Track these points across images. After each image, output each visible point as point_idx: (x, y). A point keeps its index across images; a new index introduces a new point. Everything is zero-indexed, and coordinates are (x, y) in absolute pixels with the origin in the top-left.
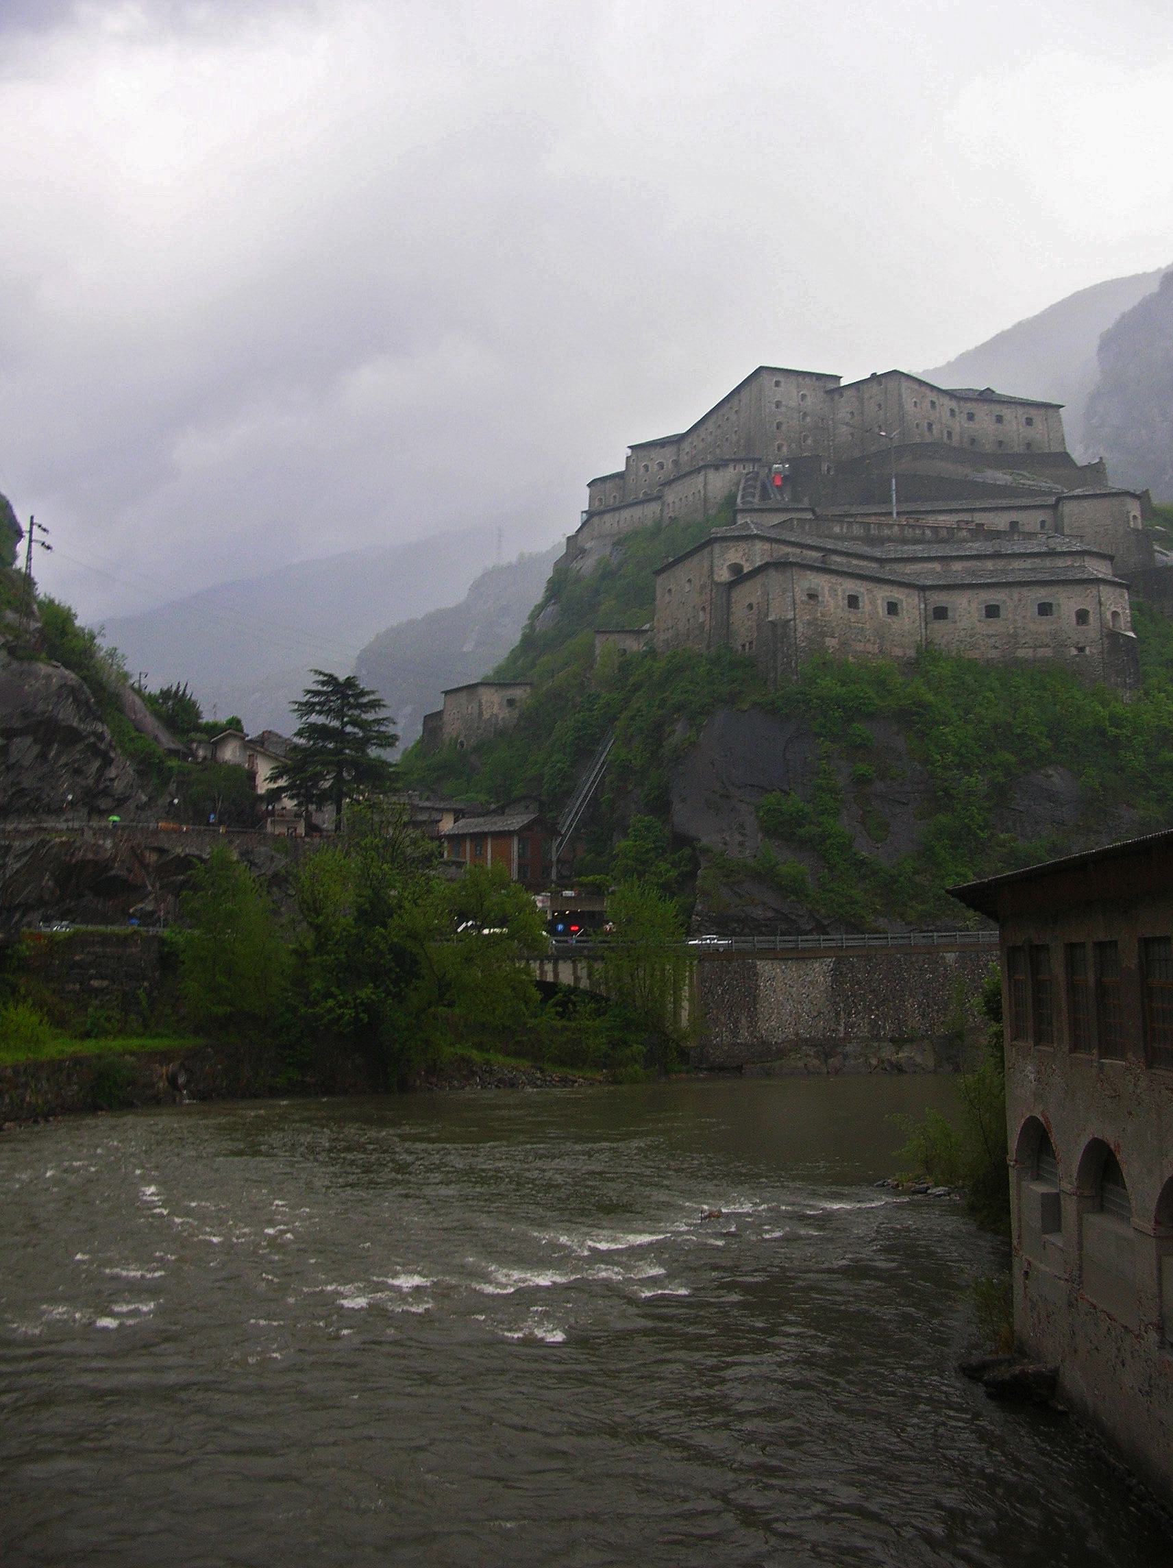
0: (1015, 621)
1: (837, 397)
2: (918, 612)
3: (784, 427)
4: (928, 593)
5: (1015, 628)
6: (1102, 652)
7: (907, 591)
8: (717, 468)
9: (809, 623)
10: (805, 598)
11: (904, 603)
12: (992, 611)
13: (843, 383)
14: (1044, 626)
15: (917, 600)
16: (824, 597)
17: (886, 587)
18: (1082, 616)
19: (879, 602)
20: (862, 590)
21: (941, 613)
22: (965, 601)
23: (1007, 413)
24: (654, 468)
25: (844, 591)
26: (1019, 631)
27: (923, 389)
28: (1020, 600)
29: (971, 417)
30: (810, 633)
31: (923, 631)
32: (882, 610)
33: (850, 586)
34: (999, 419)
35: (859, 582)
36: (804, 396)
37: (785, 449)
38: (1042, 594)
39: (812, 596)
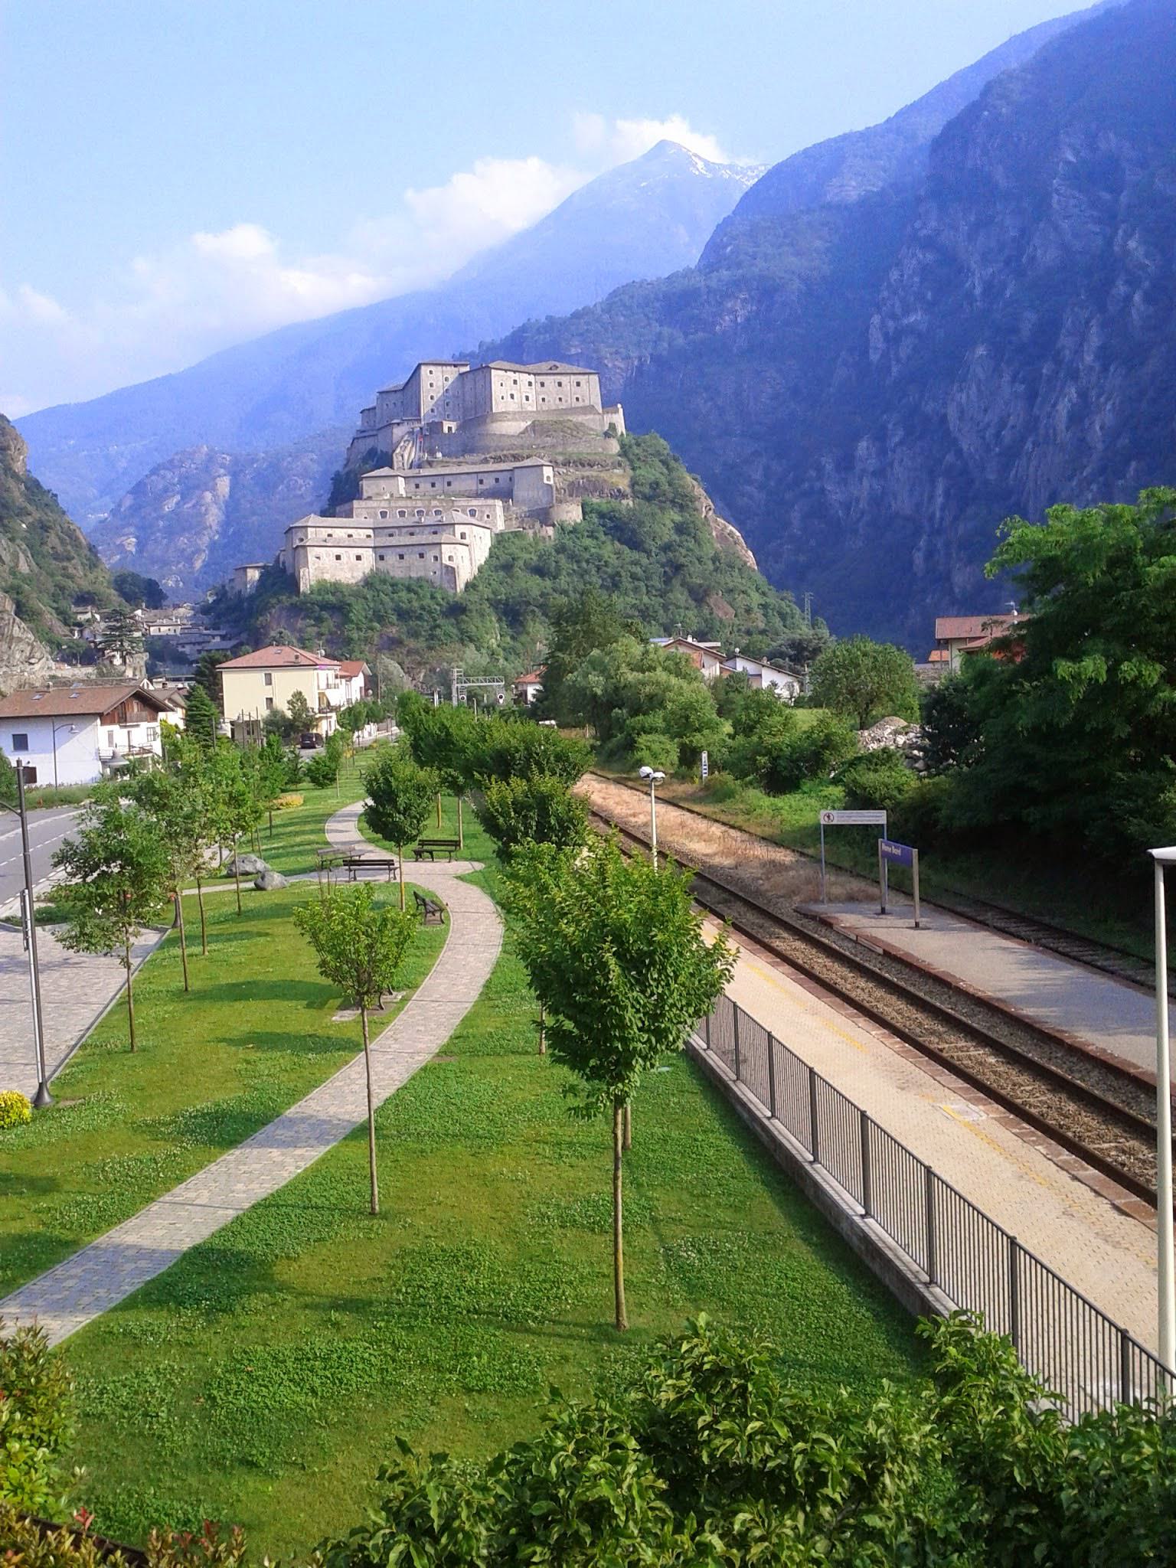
8: (398, 424)
18: (436, 558)
23: (564, 379)
24: (391, 406)
29: (542, 384)
33: (337, 551)
34: (560, 384)
38: (420, 549)
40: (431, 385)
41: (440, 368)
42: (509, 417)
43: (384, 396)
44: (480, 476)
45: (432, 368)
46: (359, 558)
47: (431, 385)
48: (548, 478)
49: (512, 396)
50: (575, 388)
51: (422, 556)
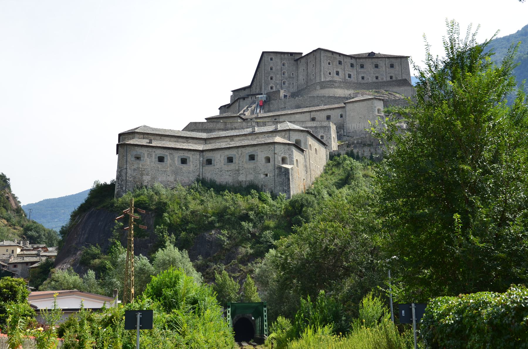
0: (239, 163)
1: (299, 62)
2: (198, 162)
3: (274, 78)
4: (204, 153)
5: (239, 166)
6: (274, 176)
7: (193, 153)
9: (135, 170)
10: (133, 159)
11: (191, 159)
12: (230, 160)
13: (303, 55)
14: (251, 165)
15: (198, 156)
16: (144, 157)
17: (181, 152)
18: (268, 160)
19: (176, 159)
20: (167, 154)
21: (209, 162)
22: (219, 156)
23: (381, 63)
25: (156, 155)
26: (240, 168)
27: (335, 55)
28: (241, 154)
30: (135, 174)
31: (201, 170)
32: (177, 162)
33: (160, 153)
34: (377, 66)
35: (165, 151)
36: (284, 65)
37: (274, 88)
38: (250, 151)
39: (138, 158)
40: (271, 69)
41: (279, 55)
42: (336, 85)
43: (236, 93)
44: (313, 115)
45: (273, 56)
46: (184, 161)
47: (271, 69)
48: (379, 110)
49: (338, 73)
50: (389, 70)
51: (252, 158)
